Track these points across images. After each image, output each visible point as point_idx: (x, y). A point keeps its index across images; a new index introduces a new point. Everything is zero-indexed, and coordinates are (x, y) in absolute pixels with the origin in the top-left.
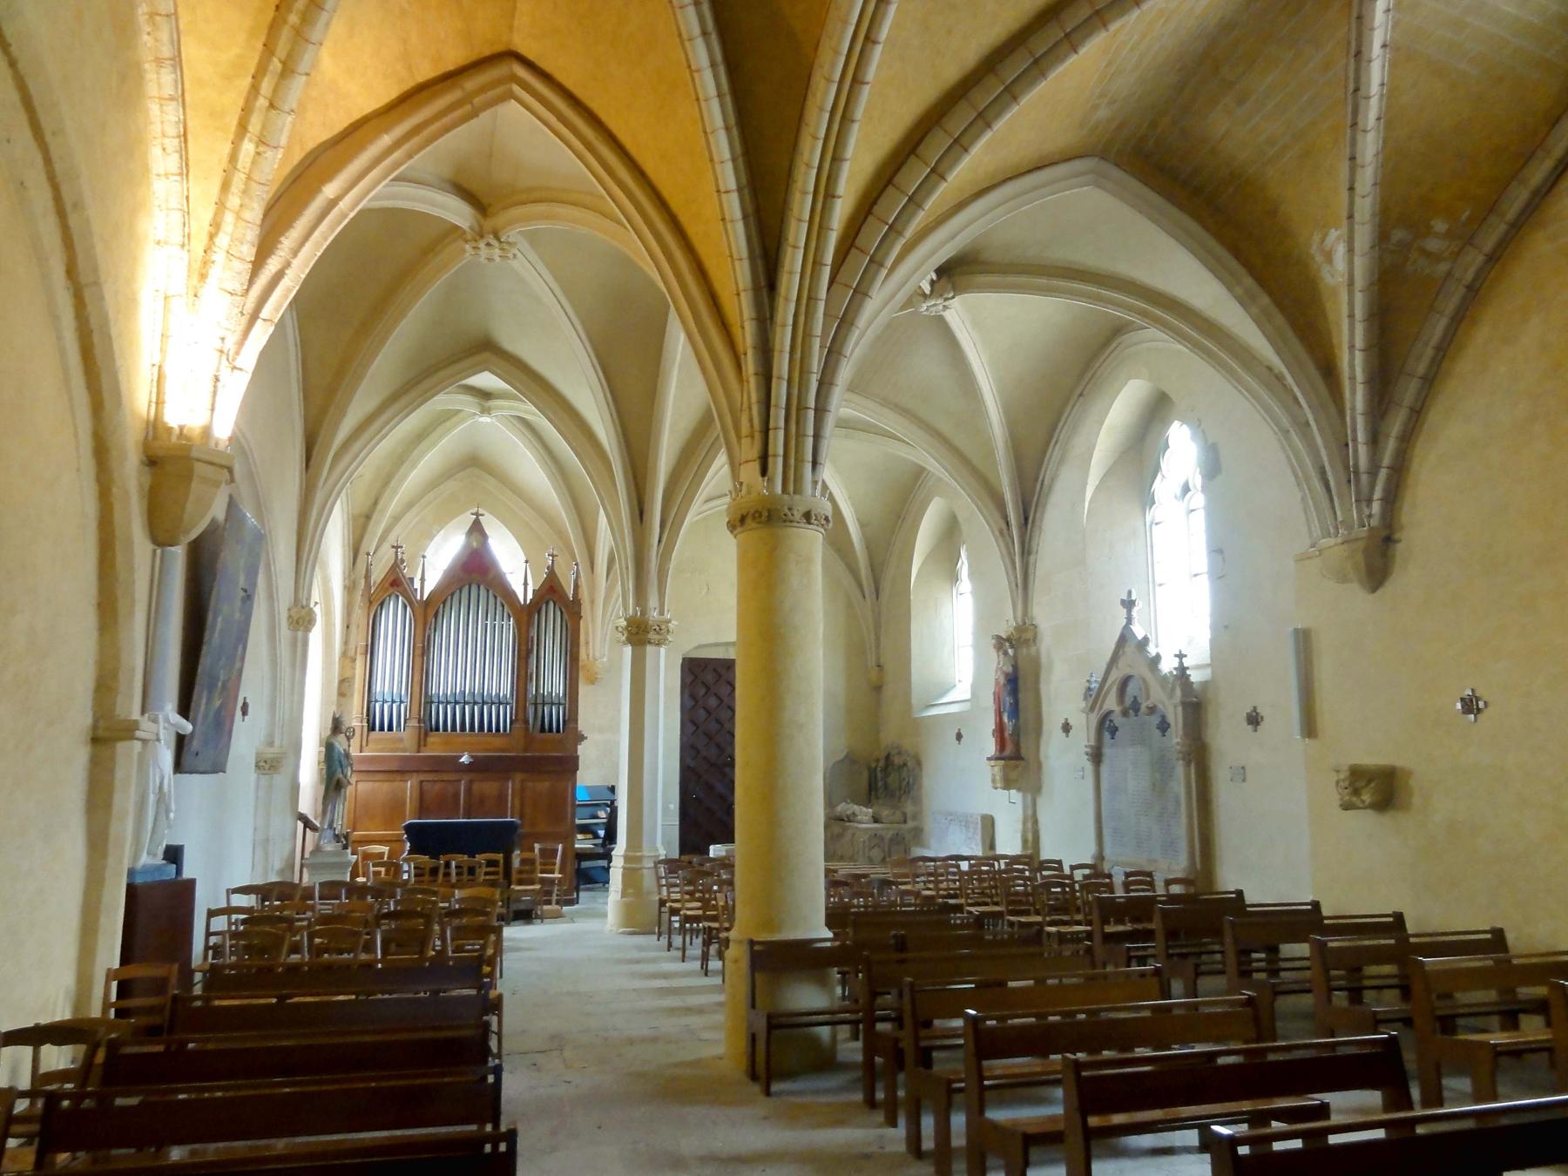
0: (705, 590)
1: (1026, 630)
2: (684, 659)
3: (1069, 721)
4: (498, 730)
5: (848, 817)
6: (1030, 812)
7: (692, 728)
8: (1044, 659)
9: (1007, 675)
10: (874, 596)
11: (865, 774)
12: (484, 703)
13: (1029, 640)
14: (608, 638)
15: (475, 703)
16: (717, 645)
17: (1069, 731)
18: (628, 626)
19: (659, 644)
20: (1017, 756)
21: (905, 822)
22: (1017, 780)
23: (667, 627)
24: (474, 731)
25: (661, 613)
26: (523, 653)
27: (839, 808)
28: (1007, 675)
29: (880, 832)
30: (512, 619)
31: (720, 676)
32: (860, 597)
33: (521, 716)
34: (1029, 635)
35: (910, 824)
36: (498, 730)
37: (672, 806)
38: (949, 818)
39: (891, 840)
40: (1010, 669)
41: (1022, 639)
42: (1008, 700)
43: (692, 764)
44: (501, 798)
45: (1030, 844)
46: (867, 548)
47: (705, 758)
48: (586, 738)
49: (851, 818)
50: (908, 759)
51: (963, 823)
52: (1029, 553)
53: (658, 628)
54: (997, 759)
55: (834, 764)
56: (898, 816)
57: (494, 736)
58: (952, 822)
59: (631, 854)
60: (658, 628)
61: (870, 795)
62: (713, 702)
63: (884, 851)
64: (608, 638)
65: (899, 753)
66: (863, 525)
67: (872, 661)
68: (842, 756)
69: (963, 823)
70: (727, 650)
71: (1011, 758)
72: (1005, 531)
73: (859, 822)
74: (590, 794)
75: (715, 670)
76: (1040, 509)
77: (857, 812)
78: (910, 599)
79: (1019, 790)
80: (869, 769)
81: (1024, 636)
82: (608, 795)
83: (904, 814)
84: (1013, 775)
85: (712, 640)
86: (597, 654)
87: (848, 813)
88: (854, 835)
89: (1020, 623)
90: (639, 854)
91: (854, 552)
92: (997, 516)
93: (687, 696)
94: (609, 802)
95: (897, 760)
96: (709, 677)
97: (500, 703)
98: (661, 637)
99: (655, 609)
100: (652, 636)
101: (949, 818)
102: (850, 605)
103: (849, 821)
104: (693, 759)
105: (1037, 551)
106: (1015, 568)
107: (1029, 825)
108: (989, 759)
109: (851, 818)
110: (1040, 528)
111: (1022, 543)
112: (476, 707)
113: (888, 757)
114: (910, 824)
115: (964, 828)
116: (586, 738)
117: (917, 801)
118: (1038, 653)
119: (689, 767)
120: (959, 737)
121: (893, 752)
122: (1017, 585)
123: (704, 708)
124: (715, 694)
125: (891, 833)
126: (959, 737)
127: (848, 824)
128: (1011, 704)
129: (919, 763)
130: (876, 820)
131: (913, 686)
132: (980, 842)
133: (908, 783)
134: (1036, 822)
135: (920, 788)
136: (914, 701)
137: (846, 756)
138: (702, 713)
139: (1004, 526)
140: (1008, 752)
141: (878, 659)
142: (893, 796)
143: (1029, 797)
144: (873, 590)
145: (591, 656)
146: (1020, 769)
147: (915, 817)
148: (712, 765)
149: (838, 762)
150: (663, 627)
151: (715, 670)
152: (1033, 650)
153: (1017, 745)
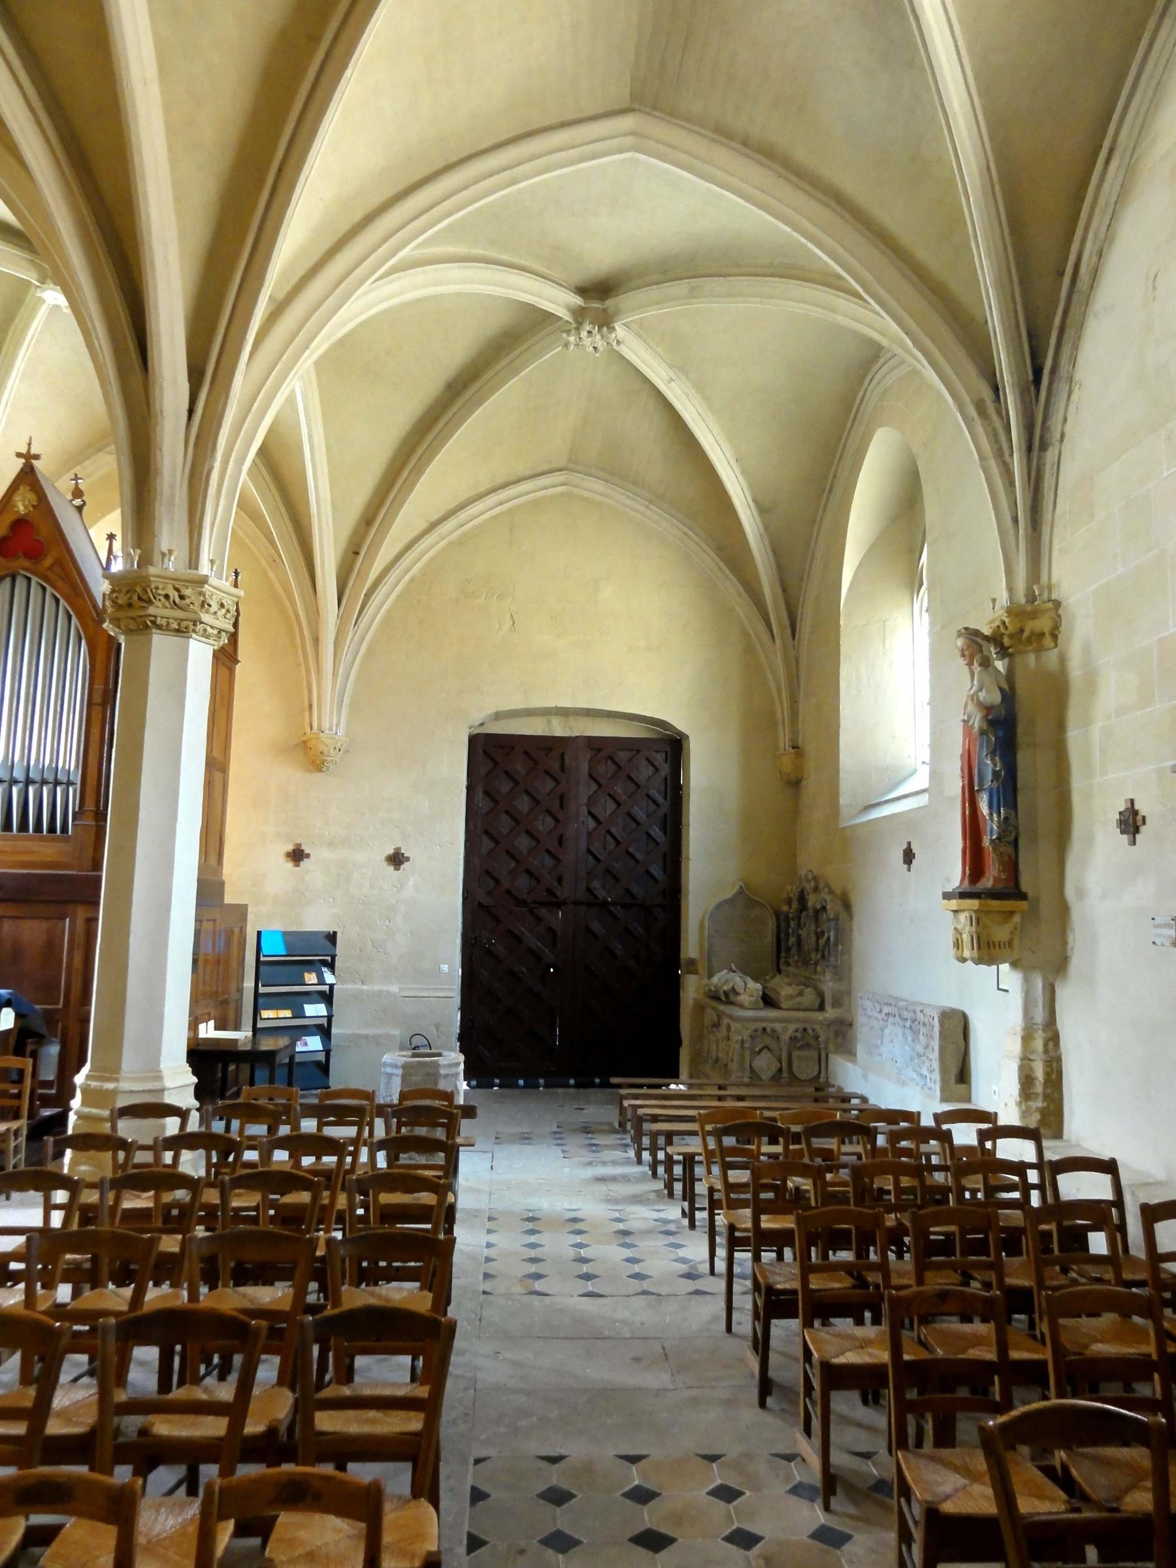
0: (509, 624)
1: (1034, 615)
2: (474, 740)
3: (1137, 807)
4: (52, 829)
5: (726, 994)
6: (1039, 1016)
7: (487, 844)
8: (1075, 672)
9: (988, 709)
10: (788, 632)
11: (771, 923)
12: (57, 783)
13: (1042, 635)
14: (346, 700)
15: (44, 782)
16: (530, 713)
17: (1137, 830)
18: (113, 591)
19: (180, 633)
20: (1011, 890)
21: (821, 1008)
22: (1010, 944)
23: (201, 594)
24: (42, 832)
25: (194, 563)
26: (98, 698)
27: (715, 979)
28: (988, 709)
29: (769, 1026)
30: (83, 642)
31: (536, 763)
32: (765, 636)
33: (90, 806)
34: (1043, 624)
35: (830, 1013)
36: (52, 829)
37: (445, 968)
38: (886, 1010)
39: (793, 1039)
40: (996, 698)
41: (1026, 634)
42: (990, 766)
43: (487, 901)
44: (51, 947)
45: (1039, 1088)
46: (774, 552)
47: (508, 892)
48: (308, 856)
49: (732, 997)
50: (828, 898)
51: (908, 1024)
52: (1044, 447)
53: (174, 595)
54: (963, 895)
55: (719, 906)
56: (809, 997)
57: (43, 839)
58: (891, 1019)
59: (93, 1084)
60: (174, 595)
61: (778, 957)
62: (523, 804)
63: (780, 1061)
64: (346, 700)
65: (816, 889)
66: (763, 509)
67: (784, 741)
68: (728, 895)
69: (908, 1024)
70: (549, 723)
71: (994, 895)
72: (991, 407)
73: (741, 1006)
74: (288, 945)
75: (526, 753)
76: (1069, 333)
77: (740, 989)
78: (839, 625)
79: (1015, 965)
80: (777, 914)
81: (1030, 626)
82: (328, 944)
83: (821, 995)
84: (1001, 933)
85: (517, 703)
86: (326, 725)
87: (725, 988)
88: (729, 1028)
89: (1022, 600)
90: (110, 1086)
91: (755, 568)
92: (972, 372)
93: (480, 794)
94: (329, 958)
95: (812, 900)
96: (520, 767)
97: (57, 783)
98: (180, 614)
99: (170, 552)
100: (157, 610)
101: (886, 1010)
102: (749, 649)
103: (729, 1002)
104: (489, 893)
105: (1063, 435)
106: (1012, 483)
107: (1039, 1044)
108: (947, 896)
109: (727, 997)
110: (1071, 379)
111: (1029, 427)
112: (45, 789)
113: (802, 898)
114: (830, 1013)
115: (908, 1032)
116: (308, 856)
117: (843, 973)
118: (1063, 660)
119: (480, 905)
120: (908, 856)
121: (809, 887)
122: (1015, 520)
123: (507, 812)
124: (527, 792)
125: (792, 1027)
126: (908, 856)
127: (722, 1008)
128: (996, 774)
129: (847, 906)
130: (768, 1001)
131: (842, 775)
132: (936, 1065)
133: (829, 939)
134: (1053, 1039)
135: (848, 951)
136: (844, 800)
137: (741, 892)
138: (505, 824)
139: (987, 394)
140: (987, 882)
141: (794, 732)
142: (806, 962)
143: (1039, 983)
144: (786, 622)
145: (315, 726)
146: (1017, 919)
147: (837, 1003)
148: (521, 903)
149: (730, 902)
150: (187, 592)
151: (526, 753)
152: (1051, 658)
153: (1012, 868)
